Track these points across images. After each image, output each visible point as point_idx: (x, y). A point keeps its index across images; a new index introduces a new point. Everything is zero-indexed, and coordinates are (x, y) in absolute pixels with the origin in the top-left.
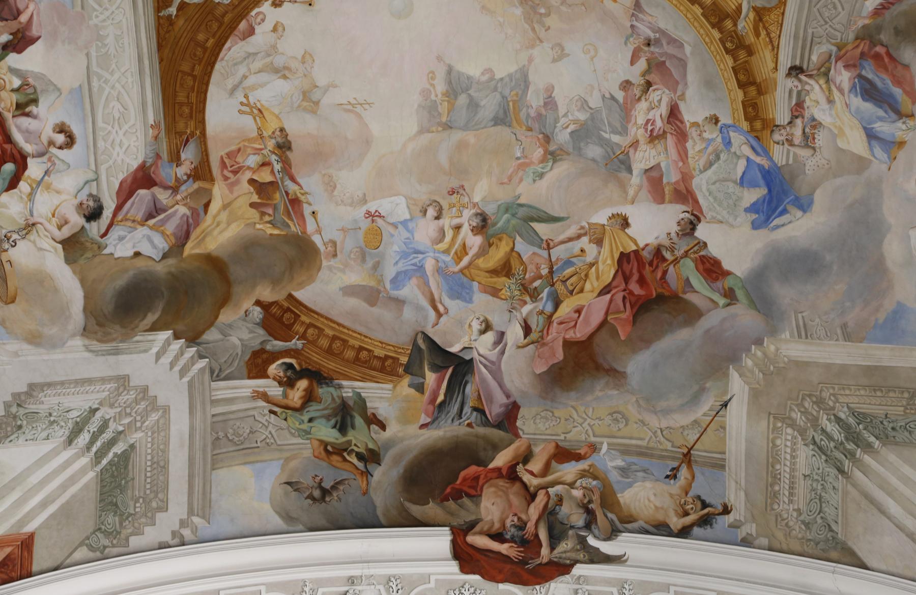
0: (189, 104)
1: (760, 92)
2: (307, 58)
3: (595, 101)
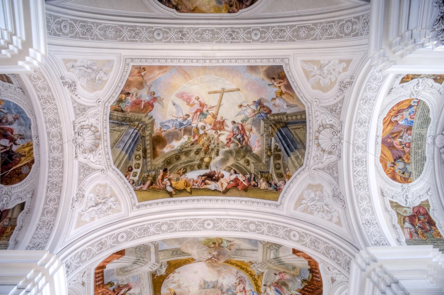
0: (158, 290)
1: (259, 287)
2: (179, 280)
3: (230, 285)
